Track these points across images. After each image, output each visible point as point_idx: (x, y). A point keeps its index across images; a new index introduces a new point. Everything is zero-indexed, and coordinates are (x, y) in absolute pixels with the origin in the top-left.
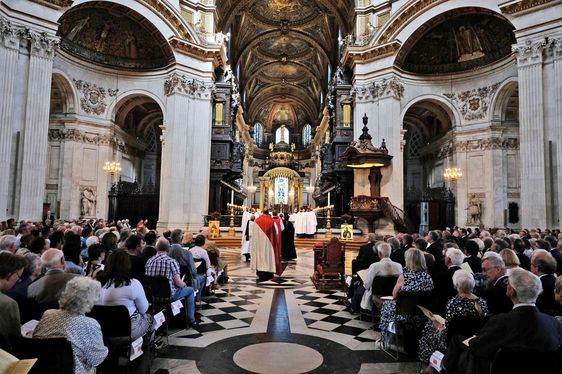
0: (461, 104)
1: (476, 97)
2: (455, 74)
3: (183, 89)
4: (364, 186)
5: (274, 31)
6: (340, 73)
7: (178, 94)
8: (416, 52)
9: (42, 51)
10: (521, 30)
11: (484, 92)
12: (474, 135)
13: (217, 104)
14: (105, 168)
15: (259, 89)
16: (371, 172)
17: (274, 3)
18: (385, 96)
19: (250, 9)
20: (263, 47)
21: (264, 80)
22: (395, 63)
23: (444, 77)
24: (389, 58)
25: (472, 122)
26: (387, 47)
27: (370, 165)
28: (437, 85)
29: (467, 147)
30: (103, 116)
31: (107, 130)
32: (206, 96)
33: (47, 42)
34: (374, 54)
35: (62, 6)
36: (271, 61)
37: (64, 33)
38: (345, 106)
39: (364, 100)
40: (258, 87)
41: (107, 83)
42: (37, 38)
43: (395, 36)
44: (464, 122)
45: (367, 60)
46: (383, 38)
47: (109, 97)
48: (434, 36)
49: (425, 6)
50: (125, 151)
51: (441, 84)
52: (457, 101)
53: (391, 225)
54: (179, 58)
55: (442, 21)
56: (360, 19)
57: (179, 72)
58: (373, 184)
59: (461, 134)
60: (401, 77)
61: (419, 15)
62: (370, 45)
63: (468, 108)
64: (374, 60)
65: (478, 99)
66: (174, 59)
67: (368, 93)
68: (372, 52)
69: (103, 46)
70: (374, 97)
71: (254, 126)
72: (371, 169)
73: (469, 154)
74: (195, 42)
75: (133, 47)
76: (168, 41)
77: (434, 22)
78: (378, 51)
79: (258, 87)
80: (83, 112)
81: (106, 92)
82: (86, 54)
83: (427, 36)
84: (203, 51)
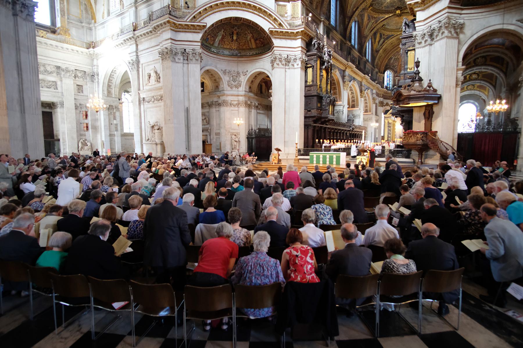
3: (280, 64)
4: (420, 122)
6: (406, 23)
7: (277, 68)
9: (194, 59)
13: (308, 69)
14: (234, 122)
15: (384, 42)
16: (426, 109)
18: (440, 38)
20: (377, 7)
27: (425, 104)
30: (241, 89)
33: (196, 54)
36: (386, 16)
37: (211, 43)
38: (409, 53)
39: (423, 44)
40: (382, 40)
42: (191, 53)
45: (426, 6)
47: (243, 76)
50: (259, 109)
53: (438, 155)
54: (276, 42)
57: (276, 51)
58: (427, 119)
60: (461, 14)
66: (273, 44)
67: (427, 38)
69: (236, 45)
70: (432, 39)
71: (384, 73)
74: (286, 28)
75: (252, 40)
76: (268, 32)
79: (382, 40)
80: (229, 88)
81: (241, 73)
82: (226, 52)
84: (293, 33)
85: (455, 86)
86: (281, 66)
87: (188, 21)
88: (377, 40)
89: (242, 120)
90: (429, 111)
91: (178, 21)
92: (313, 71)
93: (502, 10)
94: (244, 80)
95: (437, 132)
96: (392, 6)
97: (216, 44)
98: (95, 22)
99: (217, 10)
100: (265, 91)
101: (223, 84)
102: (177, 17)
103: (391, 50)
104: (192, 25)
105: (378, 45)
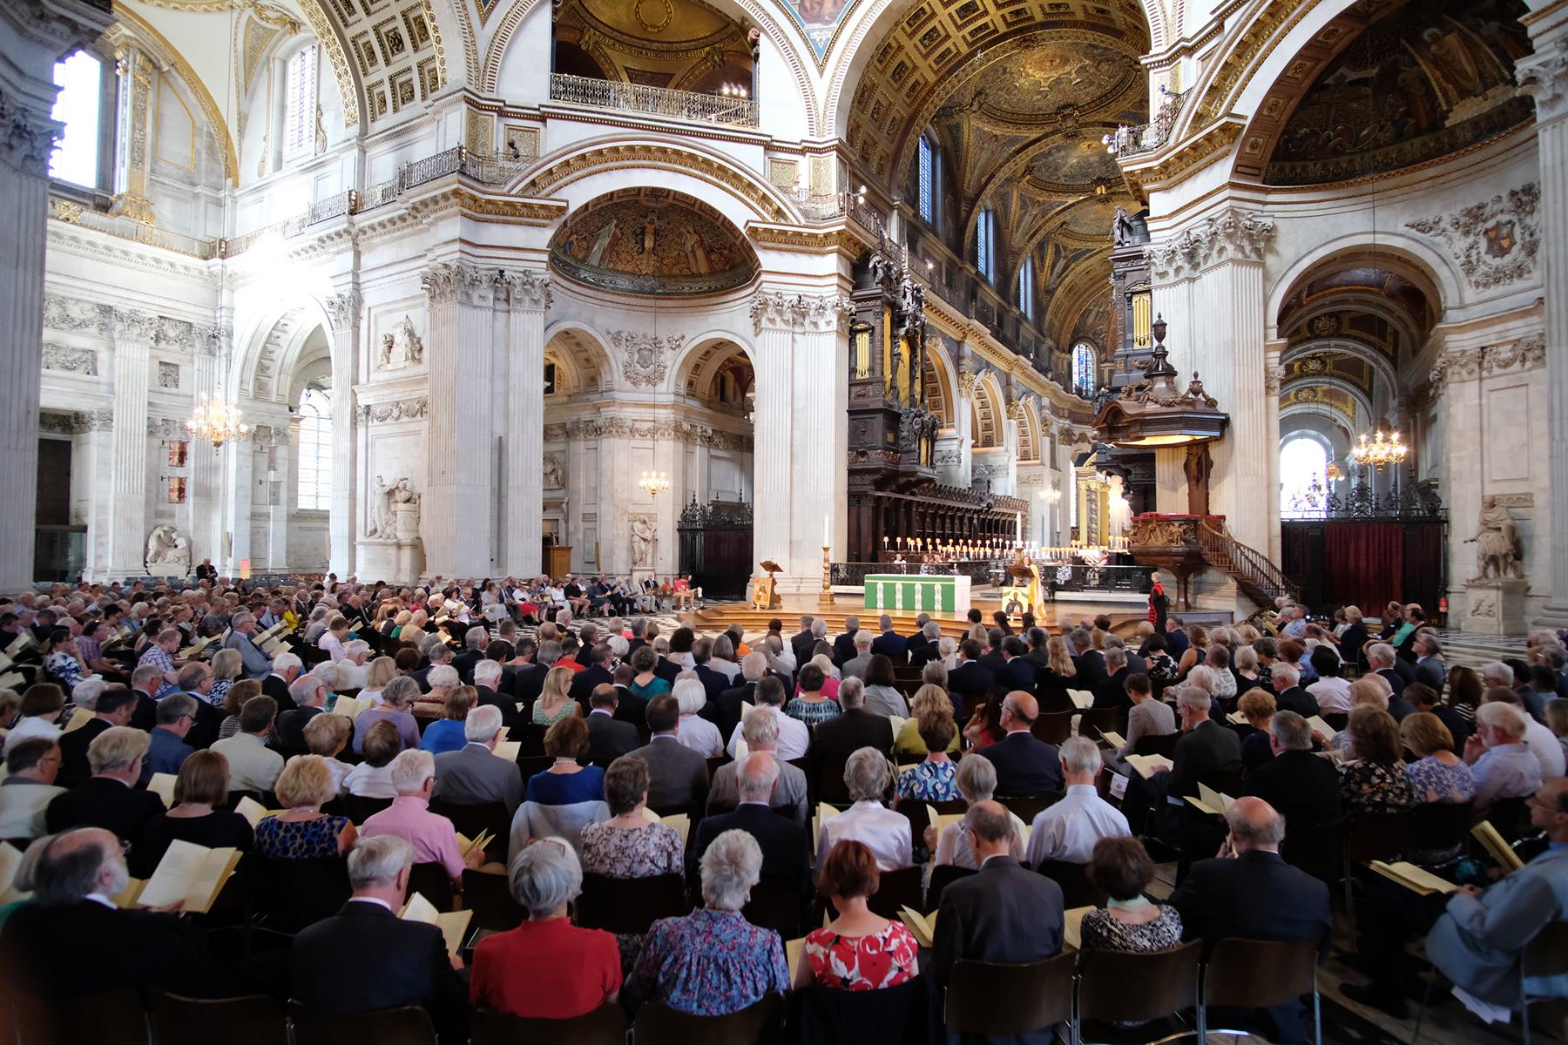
0: (1461, 243)
1: (1504, 218)
2: (1437, 164)
3: (778, 319)
4: (1175, 489)
5: (1046, 136)
6: (1122, 221)
8: (1303, 131)
9: (527, 299)
10: (1544, 10)
11: (1524, 199)
12: (1498, 328)
13: (859, 336)
14: (642, 483)
15: (1066, 268)
17: (1028, 75)
18: (1216, 262)
19: (971, 105)
20: (1043, 175)
21: (1073, 244)
22: (1236, 171)
23: (1407, 178)
24: (1222, 161)
25: (1494, 291)
26: (1209, 138)
27: (1187, 439)
28: (1385, 202)
29: (1480, 364)
30: (662, 387)
31: (669, 411)
32: (828, 323)
33: (532, 285)
34: (1185, 159)
35: (551, 219)
36: (1071, 202)
37: (580, 257)
38: (1135, 298)
39: (1171, 278)
40: (1062, 263)
41: (667, 327)
42: (518, 282)
43: (1232, 104)
44: (1471, 295)
45: (1175, 178)
46: (1199, 117)
48: (1353, 75)
49: (1294, 8)
50: (717, 445)
51: (1399, 198)
52: (1450, 239)
53: (1232, 585)
54: (768, 260)
55: (1354, 34)
56: (1157, 81)
57: (768, 285)
58: (1194, 482)
59: (1461, 329)
60: (1266, 203)
61: (1283, 35)
62: (1171, 142)
63: (1483, 254)
64: (1190, 176)
65: (1510, 222)
67: (1180, 260)
68: (1180, 156)
69: (652, 263)
70: (1195, 266)
71: (1070, 352)
72: (1189, 445)
73: (1487, 384)
74: (795, 221)
75: (700, 254)
76: (744, 231)
77: (1332, 41)
78: (1192, 153)
79: (1062, 263)
80: (628, 385)
81: (665, 343)
82: (623, 283)
83: (1330, 81)
84: (816, 236)
85: (1264, 392)
86: (780, 324)
87: (513, 192)
88: (1048, 261)
89: (666, 478)
90: (1199, 458)
91: (485, 193)
92: (872, 341)
93: (1369, 198)
94: (673, 362)
95: (1223, 517)
96: (1086, 175)
97: (594, 260)
98: (236, 185)
99: (598, 167)
100: (735, 394)
101: (611, 372)
102: (483, 183)
103: (1088, 289)
104: (524, 205)
105: (1051, 274)
